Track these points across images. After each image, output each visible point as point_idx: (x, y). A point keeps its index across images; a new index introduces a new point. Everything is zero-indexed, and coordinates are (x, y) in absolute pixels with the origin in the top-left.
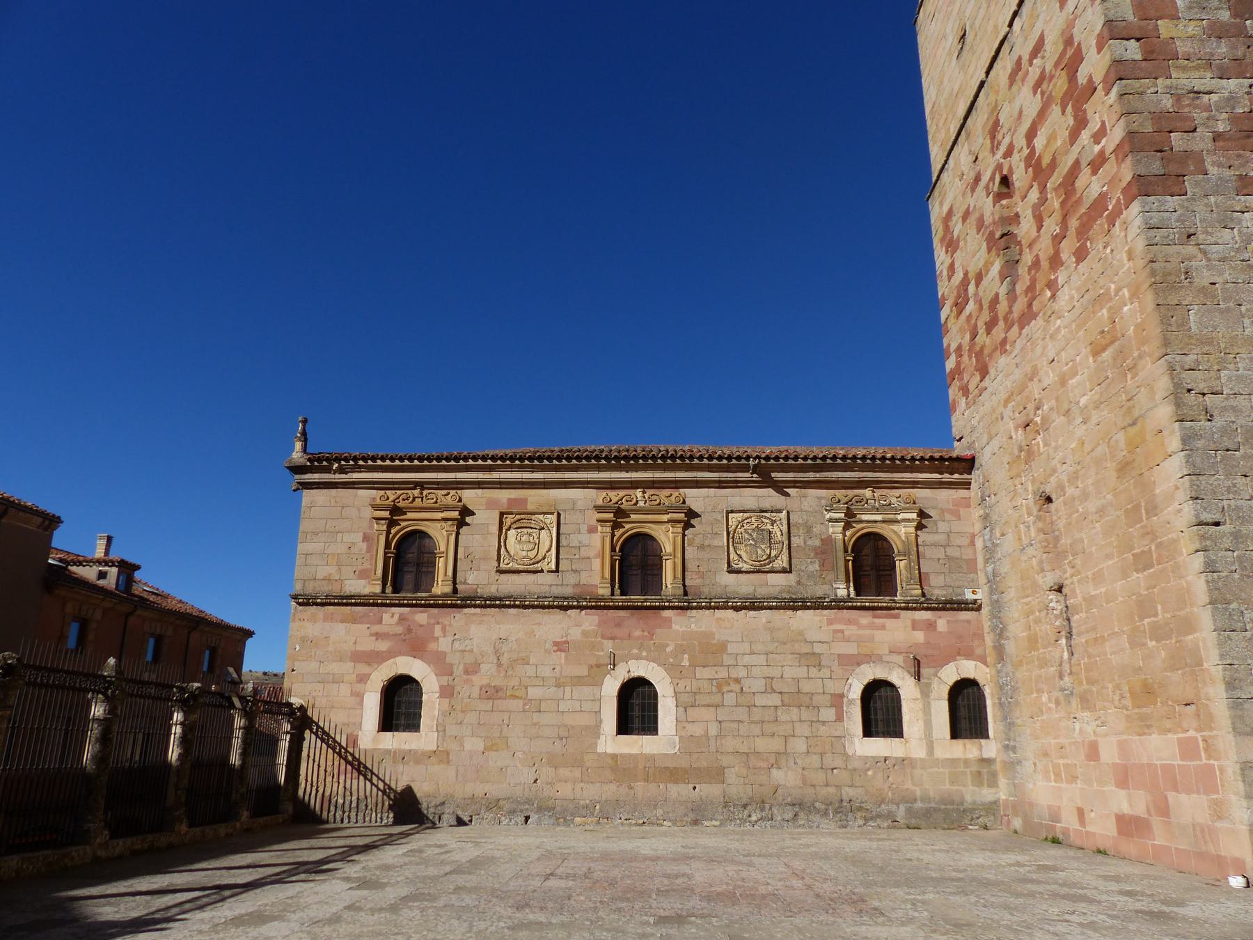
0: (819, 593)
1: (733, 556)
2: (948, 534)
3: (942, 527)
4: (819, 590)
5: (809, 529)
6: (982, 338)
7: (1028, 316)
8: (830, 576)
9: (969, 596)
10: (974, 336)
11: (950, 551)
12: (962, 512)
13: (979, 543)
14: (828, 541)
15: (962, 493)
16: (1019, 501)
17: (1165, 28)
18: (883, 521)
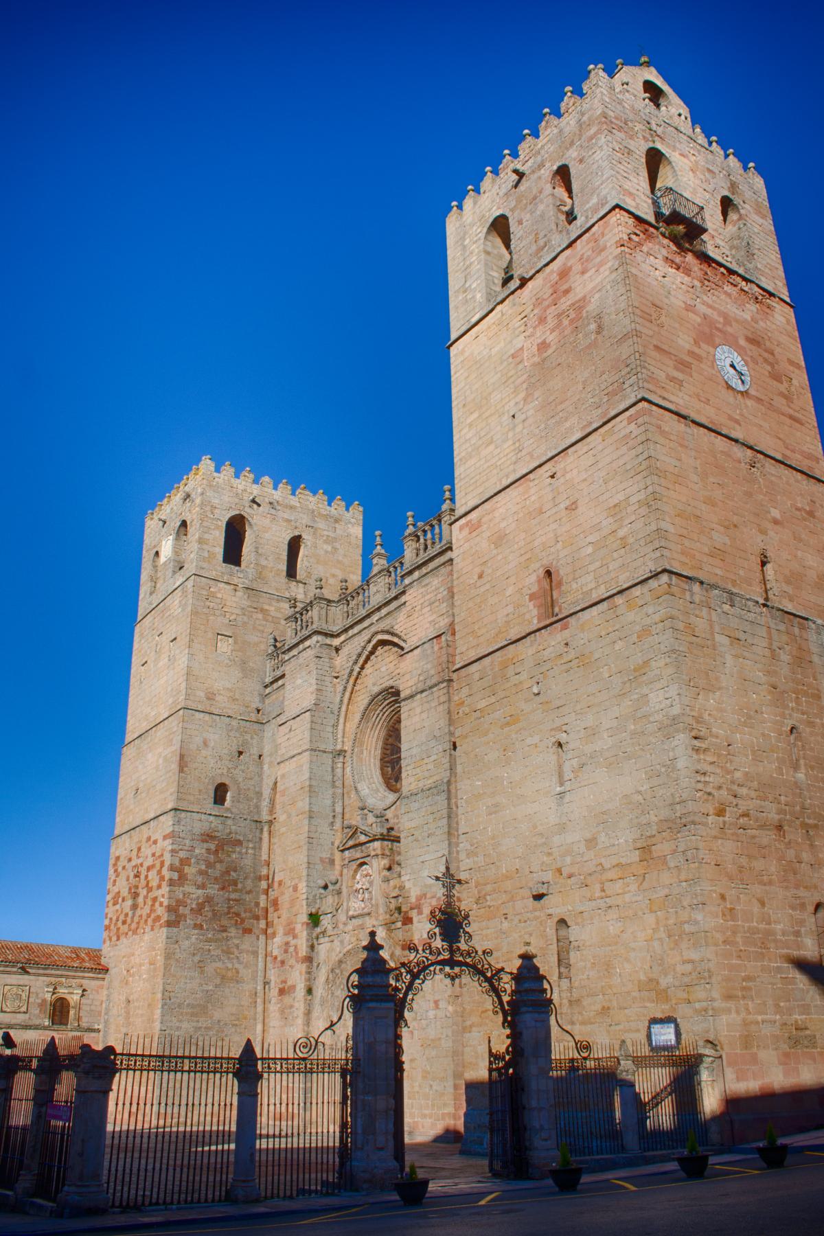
0: (37, 1023)
1: (4, 1005)
2: (93, 1000)
3: (91, 996)
4: (37, 1022)
5: (37, 994)
6: (120, 923)
7: (135, 932)
8: (42, 1016)
9: (96, 1027)
10: (117, 920)
11: (93, 1008)
12: (100, 990)
13: (104, 1005)
14: (44, 1001)
15: (101, 982)
16: (121, 997)
17: (187, 870)
18: (69, 993)
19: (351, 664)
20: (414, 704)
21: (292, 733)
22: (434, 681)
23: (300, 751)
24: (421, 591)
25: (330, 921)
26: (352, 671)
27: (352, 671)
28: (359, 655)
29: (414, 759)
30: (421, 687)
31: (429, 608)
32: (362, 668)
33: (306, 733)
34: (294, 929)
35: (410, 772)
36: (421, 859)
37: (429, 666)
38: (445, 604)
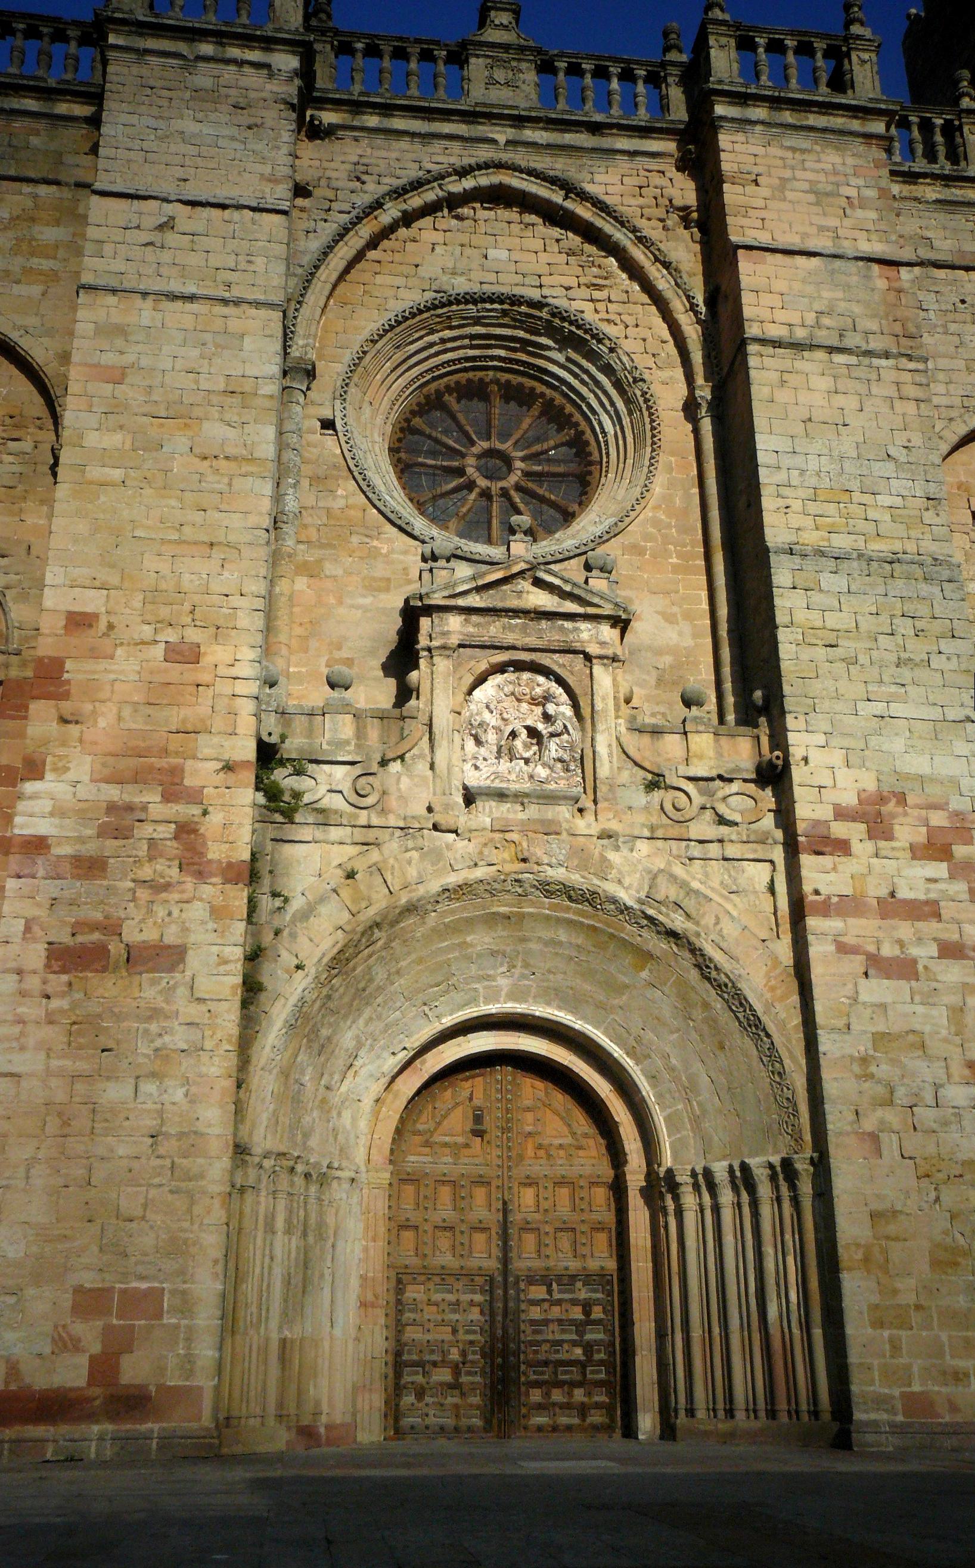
19: (373, 190)
20: (799, 365)
21: (171, 238)
22: (875, 344)
23: (227, 295)
24: (774, 151)
25: (346, 787)
26: (377, 205)
27: (377, 205)
28: (416, 185)
29: (813, 481)
30: (823, 337)
31: (812, 198)
32: (408, 219)
33: (260, 262)
34: (176, 772)
35: (797, 505)
36: (879, 708)
37: (857, 309)
38: (873, 215)
